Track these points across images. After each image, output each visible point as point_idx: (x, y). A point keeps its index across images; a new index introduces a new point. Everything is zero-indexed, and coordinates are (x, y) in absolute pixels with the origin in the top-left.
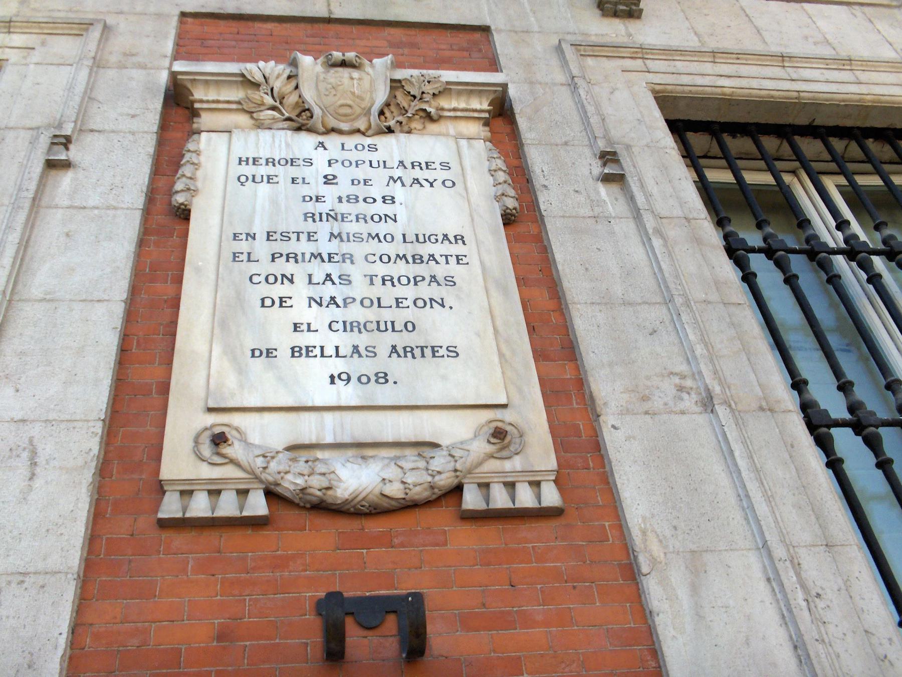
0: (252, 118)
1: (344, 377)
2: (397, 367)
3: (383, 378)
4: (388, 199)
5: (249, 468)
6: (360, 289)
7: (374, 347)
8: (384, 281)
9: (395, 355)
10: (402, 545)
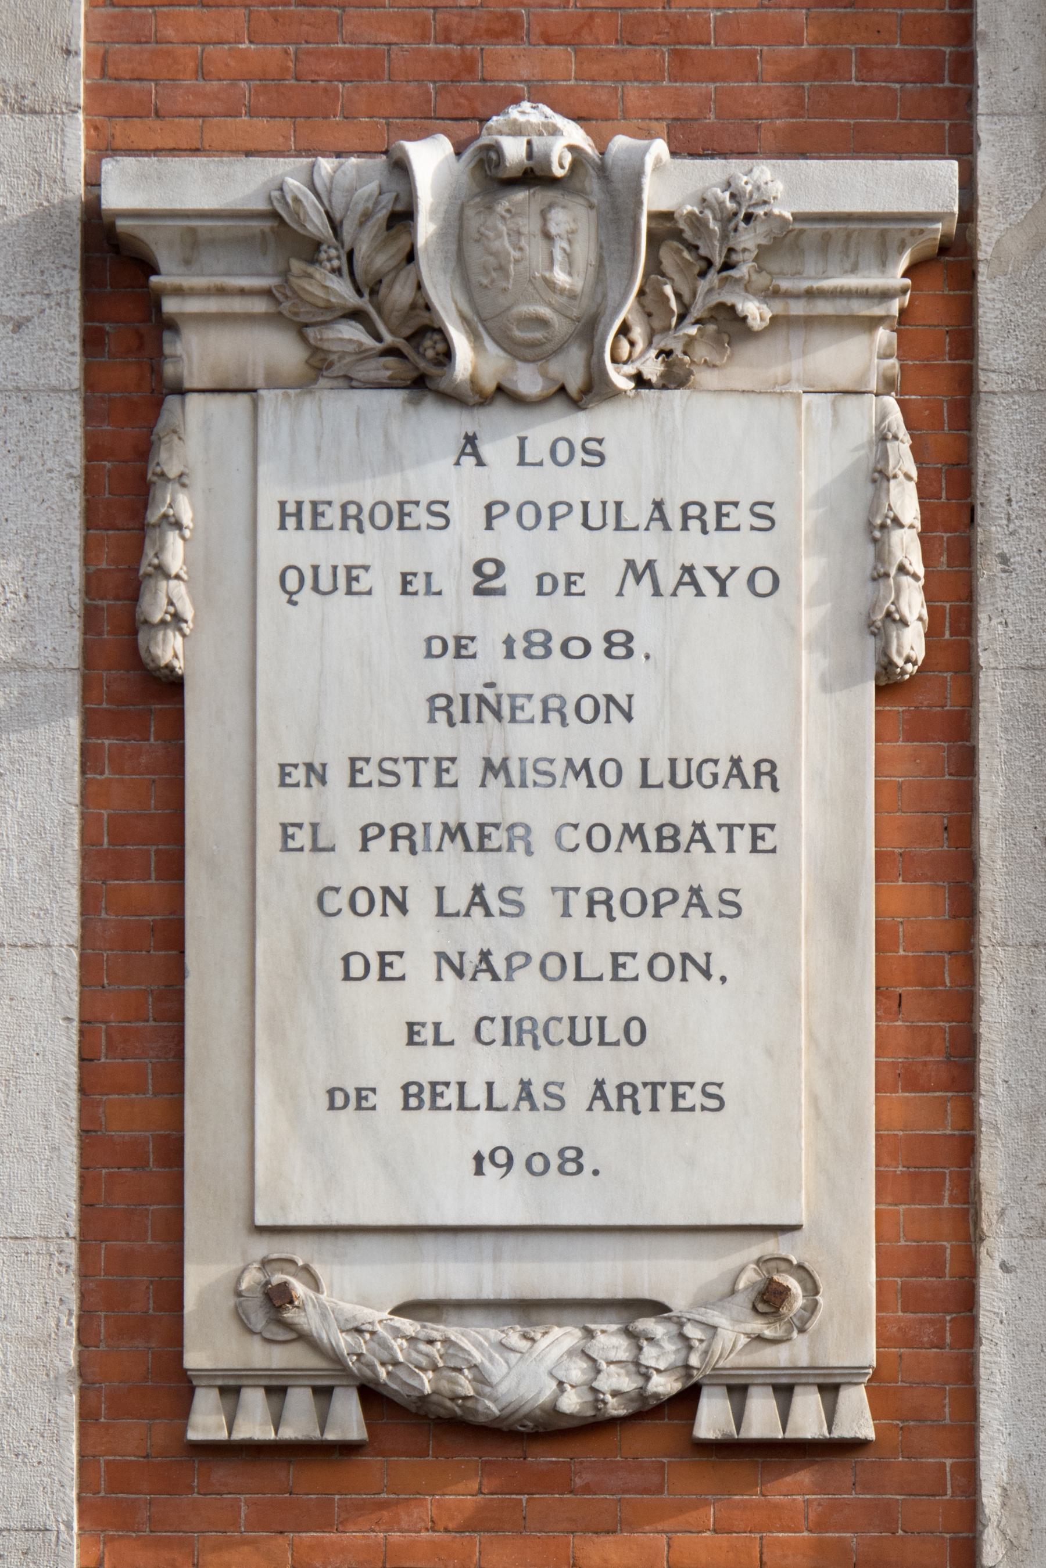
0: (304, 339)
1: (501, 1157)
2: (605, 1134)
3: (572, 1161)
4: (620, 644)
5: (331, 1353)
6: (539, 930)
7: (561, 1085)
8: (592, 902)
9: (599, 1105)
10: (587, 1489)
